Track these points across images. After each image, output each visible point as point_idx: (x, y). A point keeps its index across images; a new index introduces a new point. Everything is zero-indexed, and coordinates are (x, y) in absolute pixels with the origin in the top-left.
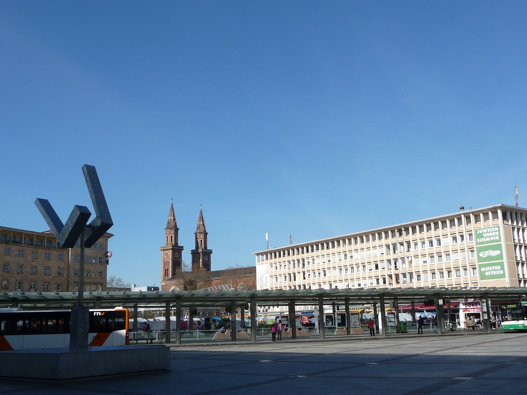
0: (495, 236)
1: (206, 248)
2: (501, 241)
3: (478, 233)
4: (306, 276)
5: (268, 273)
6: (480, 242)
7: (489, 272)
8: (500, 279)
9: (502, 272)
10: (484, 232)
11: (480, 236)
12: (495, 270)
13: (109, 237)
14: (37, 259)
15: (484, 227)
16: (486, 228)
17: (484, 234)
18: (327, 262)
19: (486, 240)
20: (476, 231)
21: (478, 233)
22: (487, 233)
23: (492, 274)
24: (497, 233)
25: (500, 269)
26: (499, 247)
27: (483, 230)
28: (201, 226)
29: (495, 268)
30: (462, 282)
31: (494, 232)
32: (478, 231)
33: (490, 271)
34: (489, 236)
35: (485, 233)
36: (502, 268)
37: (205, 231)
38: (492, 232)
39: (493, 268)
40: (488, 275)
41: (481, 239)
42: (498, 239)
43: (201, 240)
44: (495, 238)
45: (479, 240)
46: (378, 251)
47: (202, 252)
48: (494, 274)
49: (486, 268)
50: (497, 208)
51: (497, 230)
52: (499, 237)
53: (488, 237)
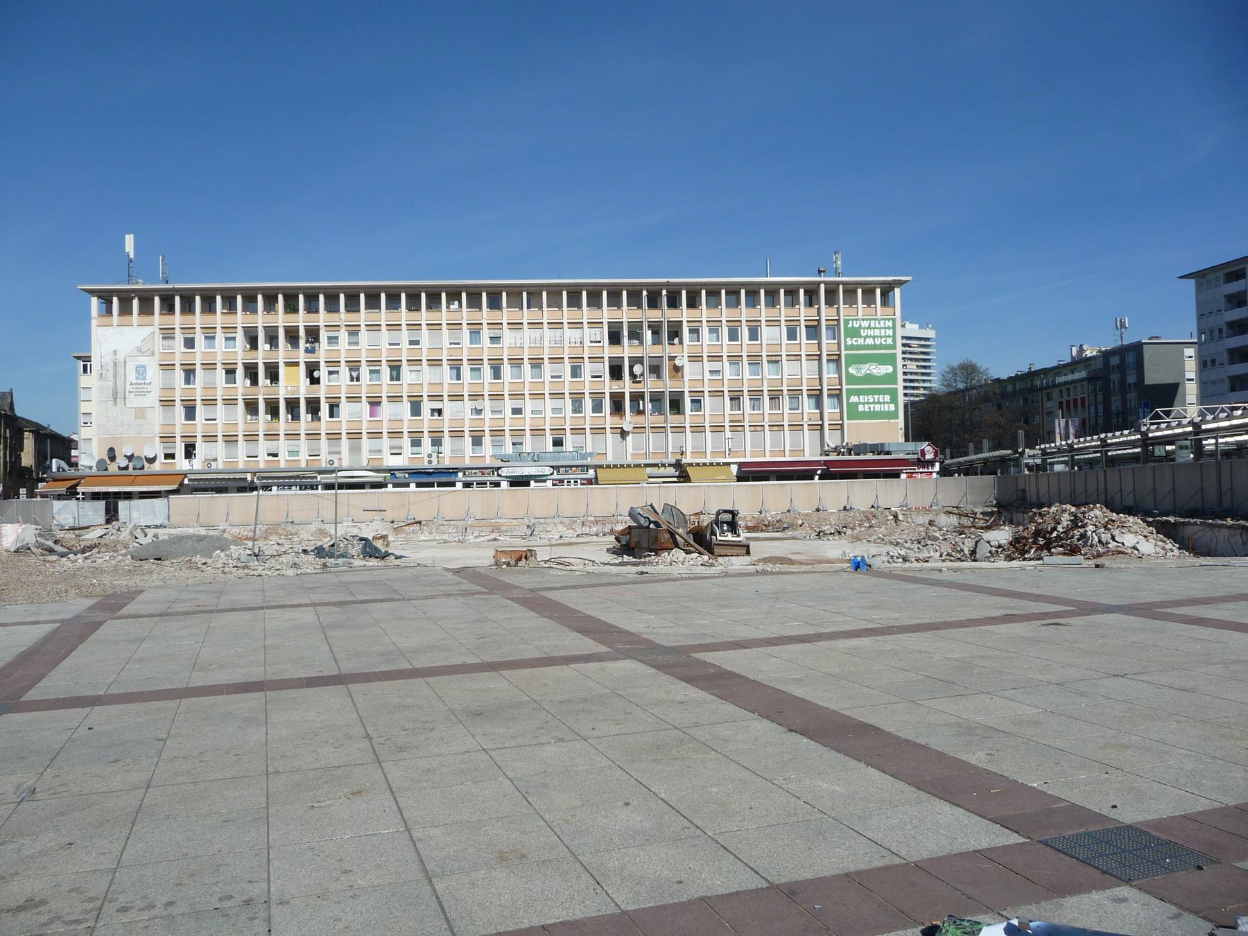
0: (886, 337)
2: (895, 349)
3: (850, 326)
4: (323, 373)
5: (153, 354)
6: (852, 344)
7: (866, 406)
8: (886, 421)
9: (892, 408)
10: (863, 326)
11: (855, 333)
12: (879, 403)
15: (864, 317)
16: (867, 320)
17: (862, 331)
18: (405, 345)
19: (866, 343)
20: (846, 322)
21: (850, 326)
22: (869, 330)
23: (872, 410)
24: (890, 332)
25: (889, 401)
26: (890, 360)
27: (861, 322)
29: (878, 399)
30: (806, 422)
31: (883, 328)
32: (851, 322)
33: (869, 403)
34: (872, 335)
35: (864, 328)
36: (894, 401)
38: (880, 328)
39: (874, 399)
40: (864, 411)
41: (856, 339)
42: (890, 344)
44: (885, 341)
45: (851, 340)
46: (588, 333)
48: (876, 410)
49: (861, 397)
50: (894, 284)
51: (891, 325)
52: (892, 341)
53: (870, 337)
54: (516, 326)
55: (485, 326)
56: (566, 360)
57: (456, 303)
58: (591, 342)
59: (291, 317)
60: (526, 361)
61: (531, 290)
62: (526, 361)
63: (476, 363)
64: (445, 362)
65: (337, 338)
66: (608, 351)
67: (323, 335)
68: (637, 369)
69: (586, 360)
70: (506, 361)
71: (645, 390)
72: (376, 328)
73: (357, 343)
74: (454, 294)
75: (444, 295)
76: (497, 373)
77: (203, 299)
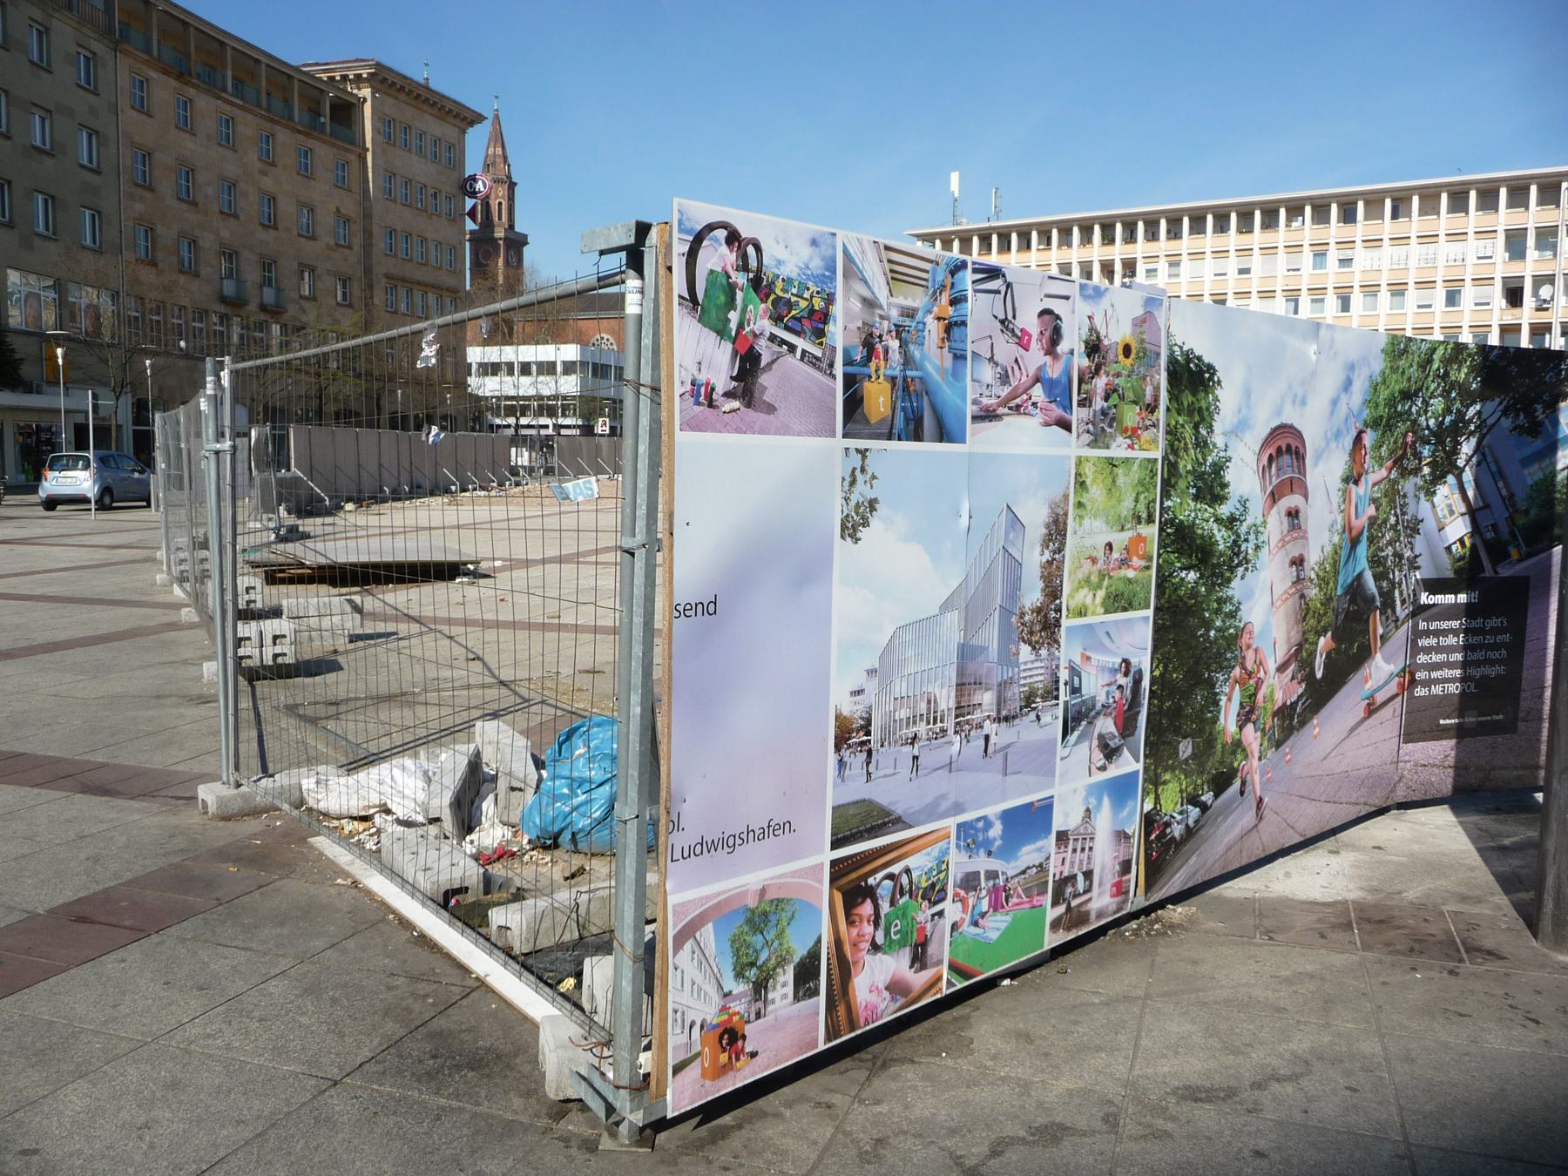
1: (511, 227)
13: (472, 123)
14: (273, 164)
18: (1232, 273)
28: (500, 160)
37: (509, 177)
43: (500, 204)
46: (1473, 247)
47: (505, 239)
54: (1373, 243)
55: (1332, 247)
56: (1440, 284)
57: (1300, 218)
58: (1479, 258)
59: (1108, 249)
60: (1384, 288)
61: (1369, 197)
62: (1384, 288)
63: (1318, 293)
64: (1279, 294)
65: (1155, 270)
66: (1503, 267)
67: (1141, 268)
68: (1545, 292)
69: (1468, 283)
70: (1357, 289)
71: (1553, 321)
72: (1200, 256)
73: (1178, 275)
74: (1295, 209)
75: (1282, 212)
76: (1345, 305)
77: (1019, 235)
